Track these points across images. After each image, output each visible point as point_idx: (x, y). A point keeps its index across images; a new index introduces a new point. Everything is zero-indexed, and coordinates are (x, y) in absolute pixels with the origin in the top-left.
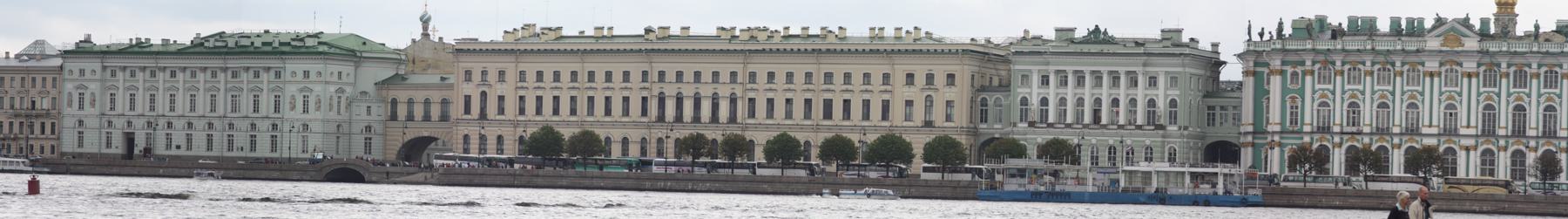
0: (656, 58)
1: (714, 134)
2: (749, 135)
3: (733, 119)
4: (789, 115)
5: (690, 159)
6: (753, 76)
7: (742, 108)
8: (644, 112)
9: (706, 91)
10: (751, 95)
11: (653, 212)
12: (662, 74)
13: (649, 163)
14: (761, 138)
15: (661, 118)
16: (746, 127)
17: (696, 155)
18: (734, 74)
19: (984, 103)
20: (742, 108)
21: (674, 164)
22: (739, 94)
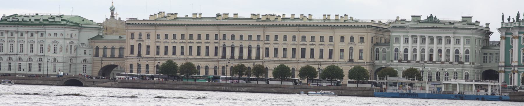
0: (222, 28)
1: (249, 64)
2: (265, 65)
3: (258, 58)
4: (285, 56)
5: (237, 76)
6: (268, 37)
7: (262, 52)
8: (216, 54)
9: (245, 44)
10: (267, 46)
11: (220, 101)
12: (224, 36)
13: (218, 78)
14: (271, 67)
15: (224, 57)
16: (264, 62)
17: (241, 75)
18: (259, 36)
19: (377, 51)
20: (262, 52)
21: (230, 79)
22: (261, 46)
